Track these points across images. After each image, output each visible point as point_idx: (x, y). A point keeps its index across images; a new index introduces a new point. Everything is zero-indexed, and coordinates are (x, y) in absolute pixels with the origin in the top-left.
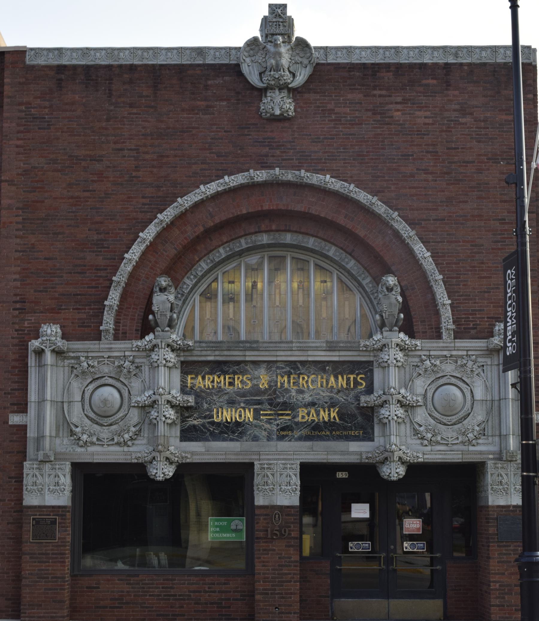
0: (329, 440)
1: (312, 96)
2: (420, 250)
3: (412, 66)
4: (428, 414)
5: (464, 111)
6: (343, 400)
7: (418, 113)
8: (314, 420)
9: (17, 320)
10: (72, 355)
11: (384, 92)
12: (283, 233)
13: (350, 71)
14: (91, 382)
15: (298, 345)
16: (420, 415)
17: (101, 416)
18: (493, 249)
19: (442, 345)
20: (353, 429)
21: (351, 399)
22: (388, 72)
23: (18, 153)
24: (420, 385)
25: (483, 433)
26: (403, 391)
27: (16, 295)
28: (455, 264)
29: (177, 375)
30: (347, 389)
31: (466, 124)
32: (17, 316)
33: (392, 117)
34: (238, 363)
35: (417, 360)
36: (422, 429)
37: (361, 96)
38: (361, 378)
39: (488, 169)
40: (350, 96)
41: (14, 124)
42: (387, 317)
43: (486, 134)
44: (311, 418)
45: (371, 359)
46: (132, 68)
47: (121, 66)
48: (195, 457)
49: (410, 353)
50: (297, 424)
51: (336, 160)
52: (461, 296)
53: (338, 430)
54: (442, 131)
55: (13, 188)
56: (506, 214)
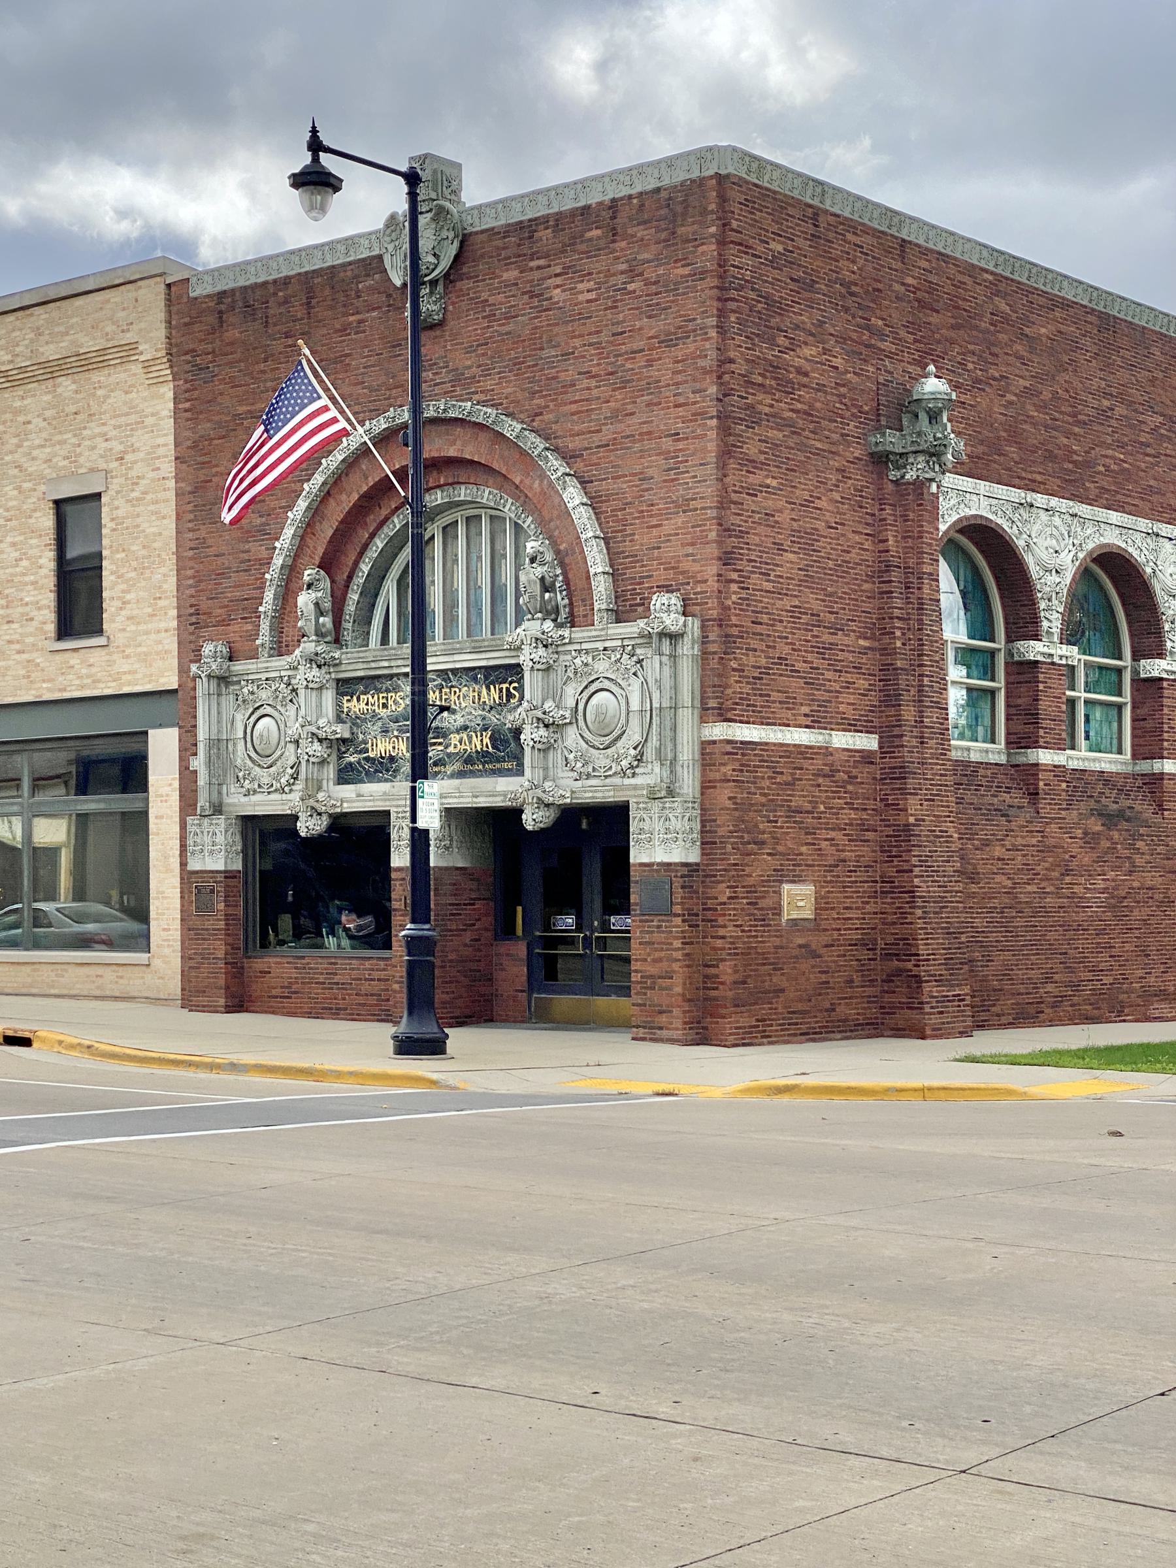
0: (481, 776)
1: (465, 285)
2: (573, 496)
3: (573, 213)
5: (633, 273)
7: (580, 286)
8: (466, 750)
9: (192, 638)
10: (235, 679)
11: (542, 262)
12: (457, 487)
13: (504, 237)
14: (252, 713)
15: (443, 647)
16: (571, 735)
17: (263, 756)
18: (665, 481)
19: (594, 633)
22: (546, 228)
23: (188, 420)
24: (571, 694)
25: (639, 759)
26: (549, 705)
27: (191, 606)
28: (621, 510)
29: (329, 696)
30: (500, 705)
31: (634, 291)
32: (193, 633)
33: (551, 298)
34: (391, 677)
35: (569, 657)
37: (516, 273)
38: (515, 688)
39: (660, 359)
40: (505, 276)
41: (181, 382)
43: (658, 304)
44: (463, 747)
46: (286, 281)
47: (275, 281)
48: (345, 805)
49: (560, 649)
50: (449, 755)
51: (490, 375)
52: (627, 557)
53: (491, 762)
54: (606, 309)
55: (184, 466)
56: (680, 425)
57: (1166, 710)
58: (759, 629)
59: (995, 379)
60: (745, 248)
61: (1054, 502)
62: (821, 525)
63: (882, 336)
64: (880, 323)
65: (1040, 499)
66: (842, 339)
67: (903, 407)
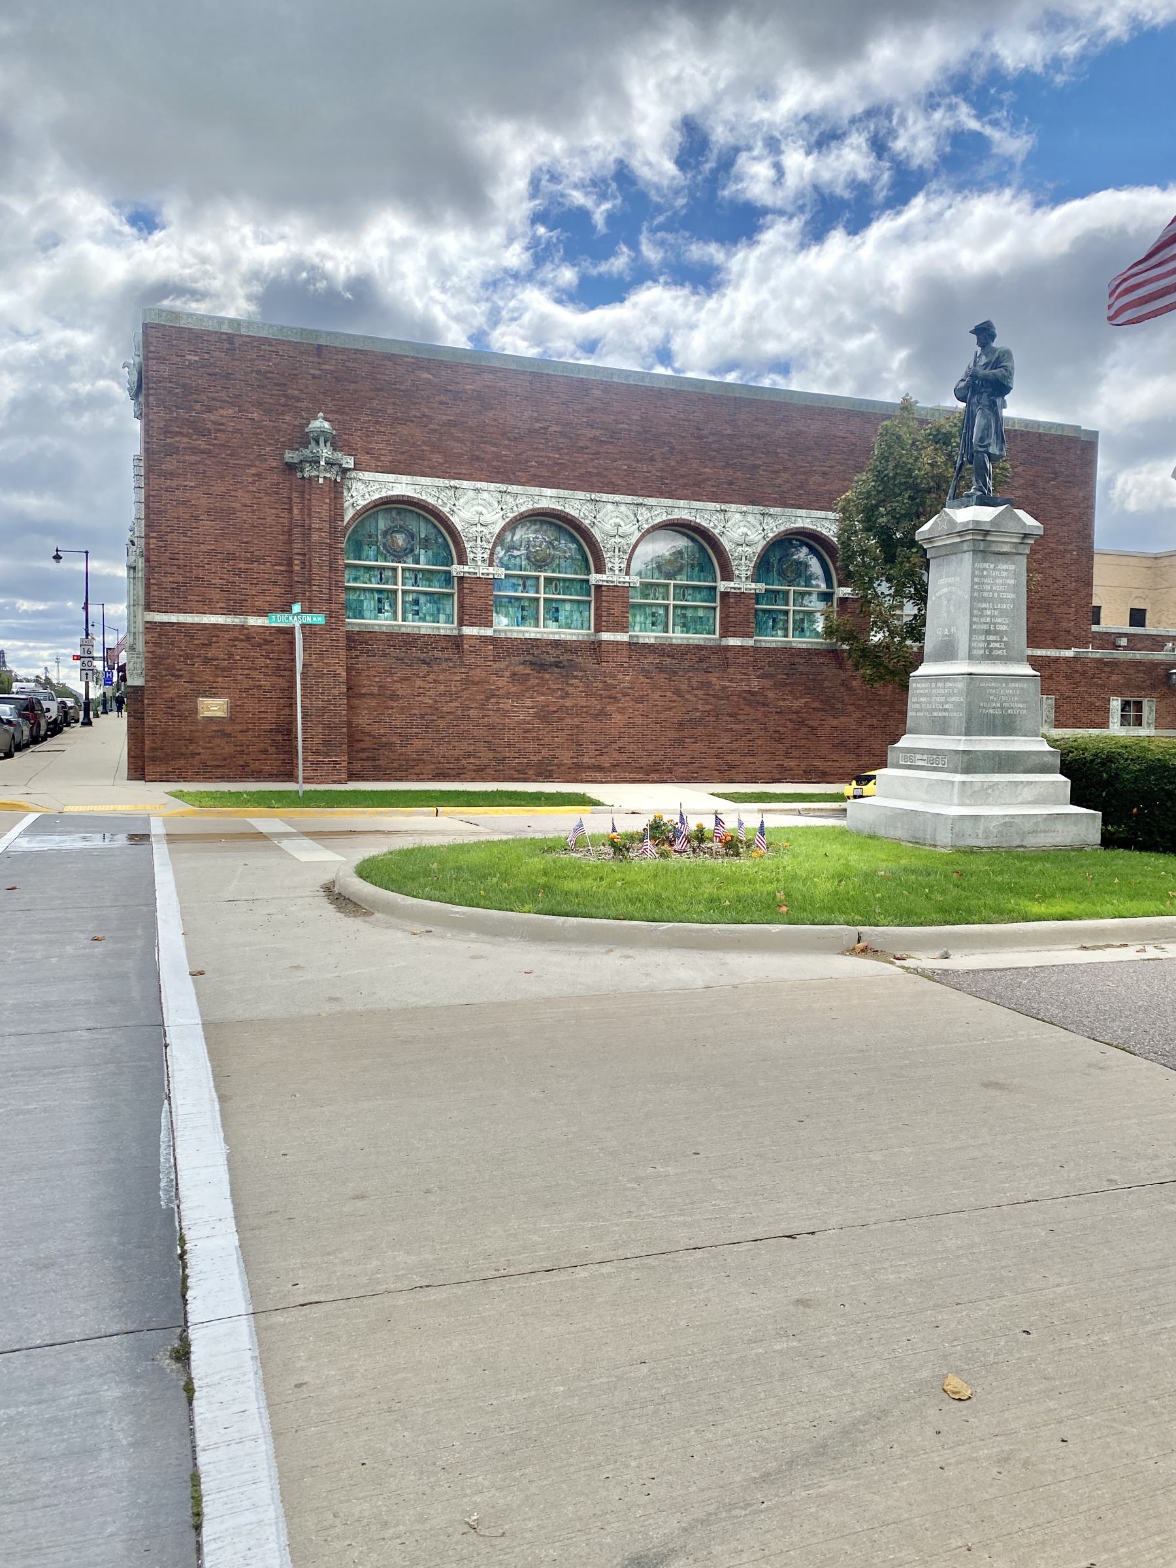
57: (605, 604)
58: (176, 562)
59: (415, 417)
60: (162, 360)
61: (479, 485)
62: (237, 505)
63: (298, 400)
64: (296, 392)
65: (465, 484)
66: (259, 404)
67: (305, 440)
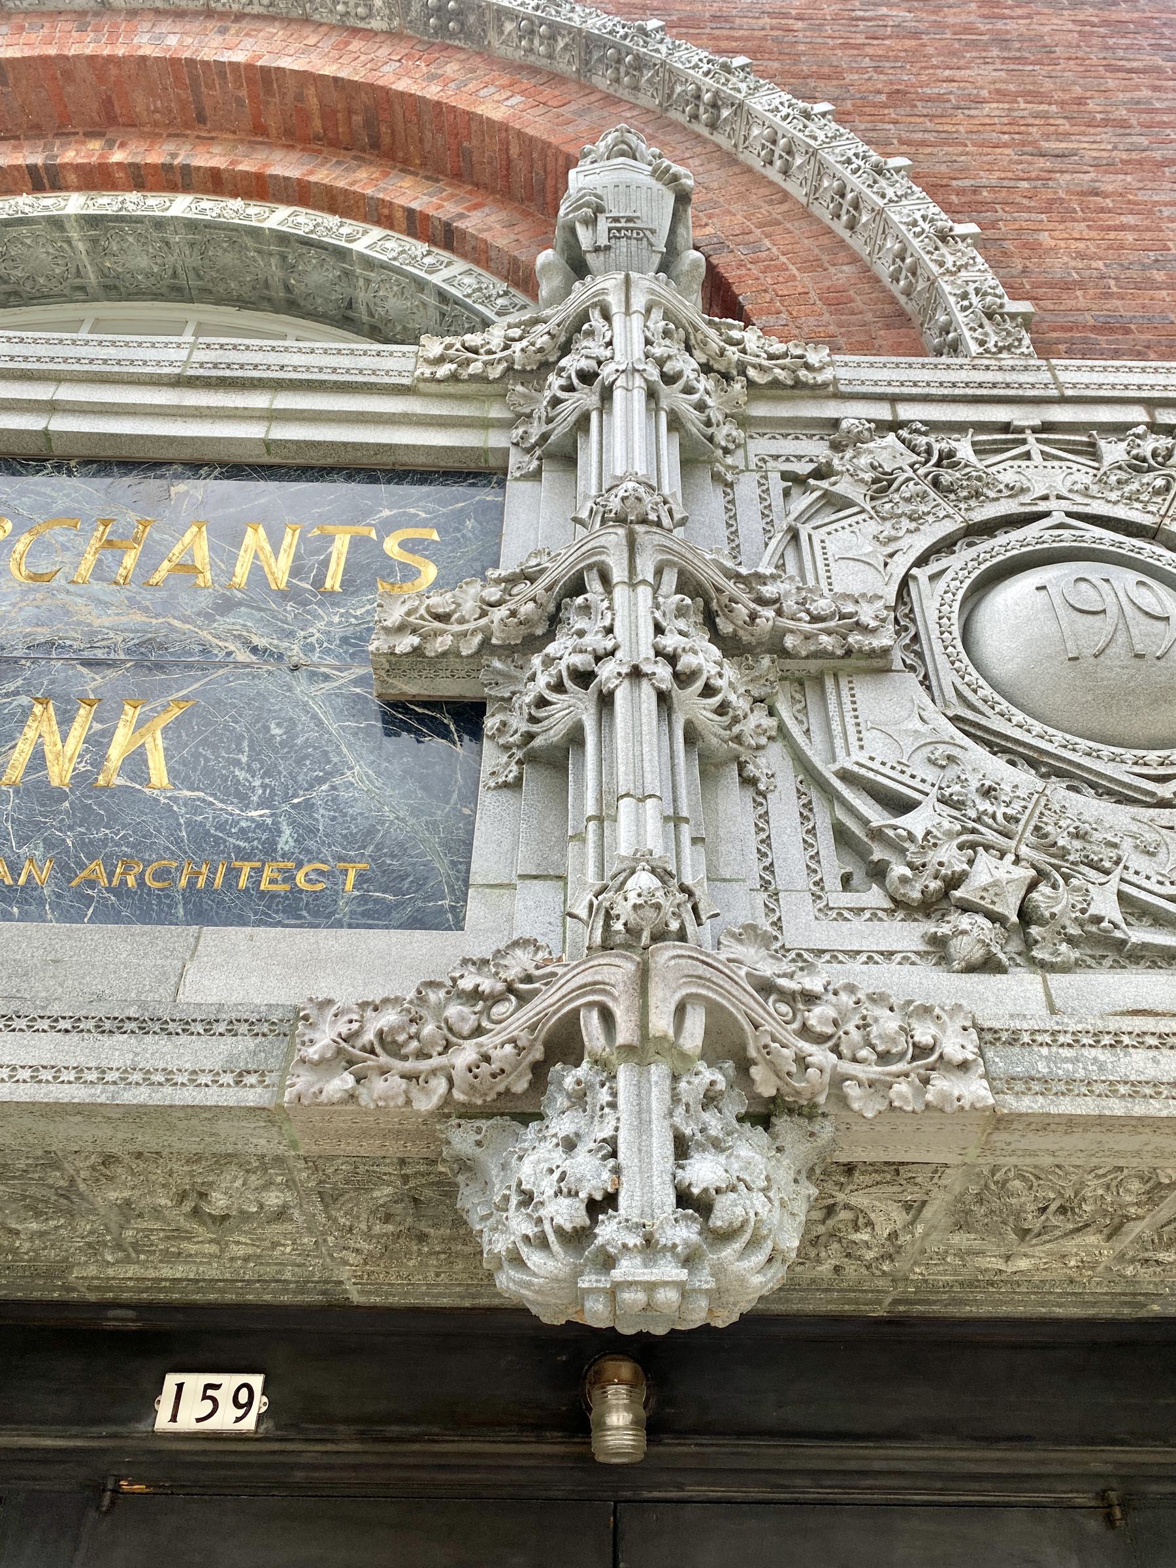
4: (956, 720)
6: (243, 656)
20: (286, 840)
21: (309, 648)
30: (289, 594)
36: (915, 822)
42: (603, 241)
45: (496, 440)
49: (760, 410)
